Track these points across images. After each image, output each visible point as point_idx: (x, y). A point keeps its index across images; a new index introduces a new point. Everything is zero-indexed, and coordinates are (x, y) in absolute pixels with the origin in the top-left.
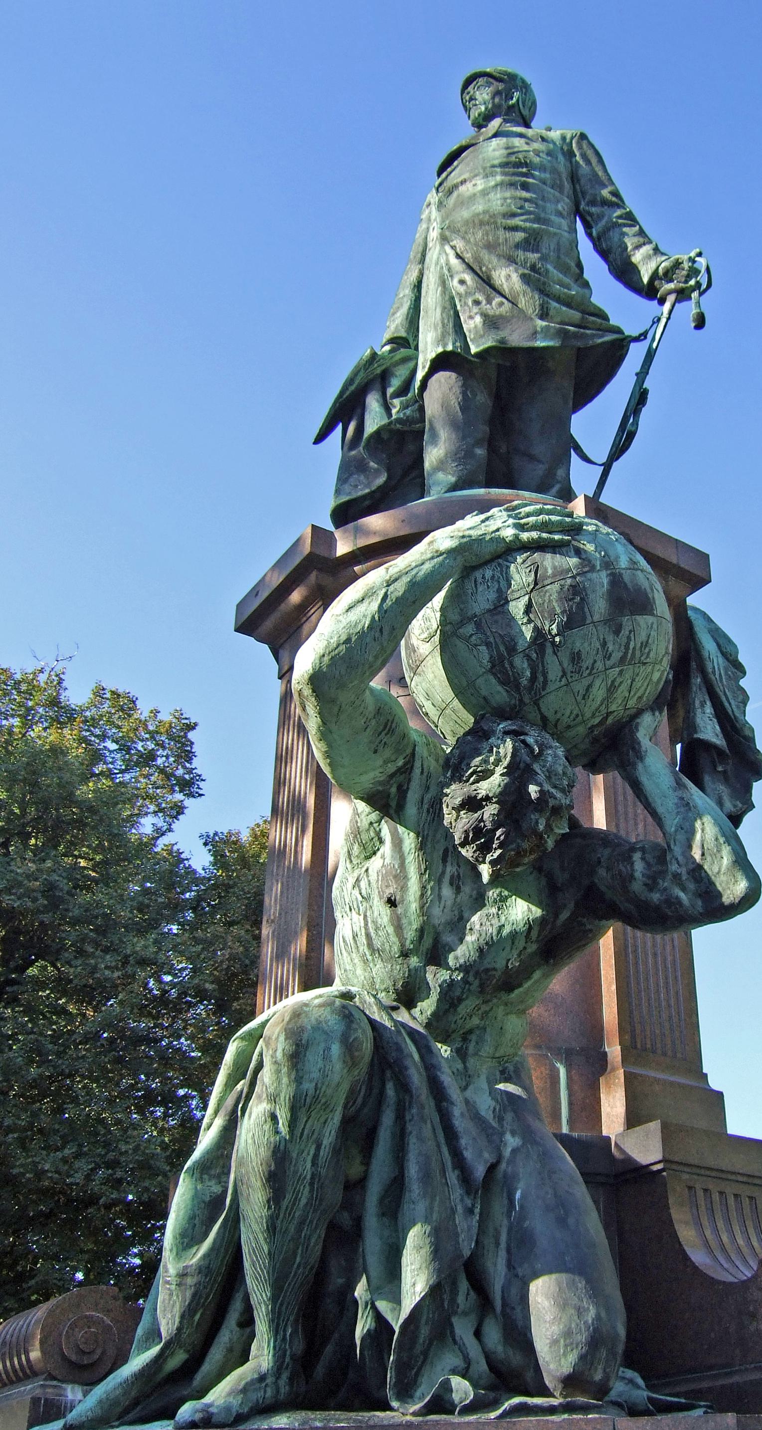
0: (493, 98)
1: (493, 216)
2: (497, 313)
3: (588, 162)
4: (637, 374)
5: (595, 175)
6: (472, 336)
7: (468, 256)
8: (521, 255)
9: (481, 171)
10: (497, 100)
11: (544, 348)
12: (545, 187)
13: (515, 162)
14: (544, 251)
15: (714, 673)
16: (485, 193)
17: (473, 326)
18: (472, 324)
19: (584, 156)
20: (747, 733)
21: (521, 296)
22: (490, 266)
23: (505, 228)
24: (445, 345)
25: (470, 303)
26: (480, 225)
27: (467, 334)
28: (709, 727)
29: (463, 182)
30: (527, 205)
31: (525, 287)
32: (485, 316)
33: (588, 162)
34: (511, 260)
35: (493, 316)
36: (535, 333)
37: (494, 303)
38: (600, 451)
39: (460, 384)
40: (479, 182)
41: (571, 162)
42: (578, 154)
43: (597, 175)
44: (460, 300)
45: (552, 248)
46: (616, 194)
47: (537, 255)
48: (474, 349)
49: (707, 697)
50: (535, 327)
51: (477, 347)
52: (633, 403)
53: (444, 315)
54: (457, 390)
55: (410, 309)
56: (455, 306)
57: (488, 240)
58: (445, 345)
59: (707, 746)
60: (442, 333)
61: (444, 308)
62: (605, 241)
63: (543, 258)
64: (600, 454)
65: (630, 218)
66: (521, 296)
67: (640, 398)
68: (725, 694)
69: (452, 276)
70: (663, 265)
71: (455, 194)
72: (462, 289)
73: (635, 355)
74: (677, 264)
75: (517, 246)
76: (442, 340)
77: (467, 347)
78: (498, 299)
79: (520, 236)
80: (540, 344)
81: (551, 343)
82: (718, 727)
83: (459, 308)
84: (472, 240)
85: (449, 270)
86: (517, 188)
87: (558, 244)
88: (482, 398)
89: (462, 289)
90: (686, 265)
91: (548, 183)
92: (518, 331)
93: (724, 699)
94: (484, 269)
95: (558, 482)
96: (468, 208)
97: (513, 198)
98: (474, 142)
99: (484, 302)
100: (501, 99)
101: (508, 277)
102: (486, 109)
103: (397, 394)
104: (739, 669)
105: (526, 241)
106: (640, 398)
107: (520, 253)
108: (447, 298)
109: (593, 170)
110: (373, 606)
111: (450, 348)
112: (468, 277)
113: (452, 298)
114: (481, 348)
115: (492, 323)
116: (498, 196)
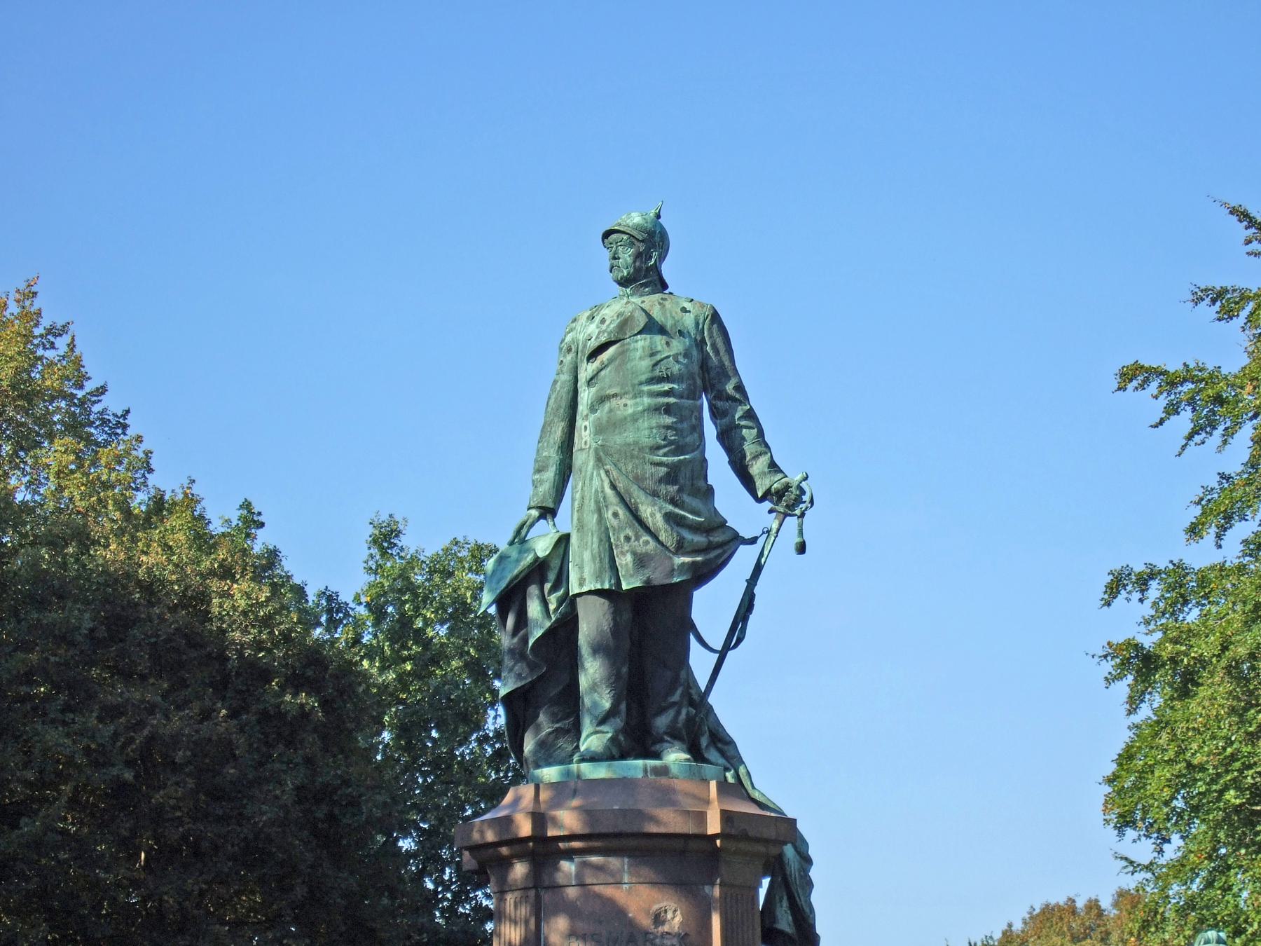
0: (634, 262)
1: (641, 449)
2: (644, 551)
3: (717, 352)
4: (747, 580)
5: (722, 365)
6: (624, 573)
7: (620, 486)
8: (663, 489)
9: (631, 389)
10: (638, 264)
11: (679, 582)
12: (683, 401)
13: (659, 377)
14: (682, 481)
15: (791, 876)
16: (635, 418)
17: (624, 562)
18: (625, 561)
19: (714, 346)
20: (811, 922)
21: (663, 532)
22: (638, 500)
23: (651, 464)
24: (602, 583)
25: (622, 539)
26: (631, 458)
27: (619, 568)
28: (785, 919)
29: (615, 395)
30: (669, 433)
31: (666, 526)
32: (634, 554)
33: (717, 352)
34: (655, 494)
35: (641, 554)
36: (673, 570)
37: (641, 541)
39: (612, 610)
40: (629, 402)
41: (702, 352)
42: (709, 344)
43: (724, 365)
44: (614, 534)
45: (687, 476)
46: (740, 388)
47: (676, 487)
48: (625, 587)
49: (785, 893)
50: (673, 565)
51: (628, 584)
52: (743, 610)
53: (601, 548)
54: (609, 617)
55: (556, 474)
56: (610, 538)
57: (637, 473)
58: (602, 583)
59: (782, 932)
60: (600, 568)
61: (601, 540)
62: (728, 438)
63: (680, 491)
65: (751, 415)
66: (663, 532)
68: (797, 892)
69: (607, 507)
70: (775, 485)
71: (607, 406)
72: (615, 522)
74: (787, 487)
75: (661, 481)
76: (599, 577)
77: (619, 583)
78: (646, 538)
79: (663, 470)
80: (676, 580)
81: (684, 578)
82: (790, 918)
83: (612, 540)
84: (623, 469)
85: (604, 498)
86: (660, 413)
87: (692, 471)
88: (627, 616)
89: (615, 522)
91: (685, 395)
92: (660, 568)
93: (796, 895)
94: (633, 500)
95: (681, 685)
96: (620, 433)
97: (659, 427)
98: (621, 337)
99: (633, 538)
100: (641, 262)
101: (653, 515)
102: (628, 274)
104: (807, 861)
105: (668, 474)
107: (663, 487)
108: (603, 529)
109: (721, 361)
111: (607, 586)
112: (621, 512)
113: (607, 529)
114: (631, 587)
115: (641, 561)
116: (646, 424)
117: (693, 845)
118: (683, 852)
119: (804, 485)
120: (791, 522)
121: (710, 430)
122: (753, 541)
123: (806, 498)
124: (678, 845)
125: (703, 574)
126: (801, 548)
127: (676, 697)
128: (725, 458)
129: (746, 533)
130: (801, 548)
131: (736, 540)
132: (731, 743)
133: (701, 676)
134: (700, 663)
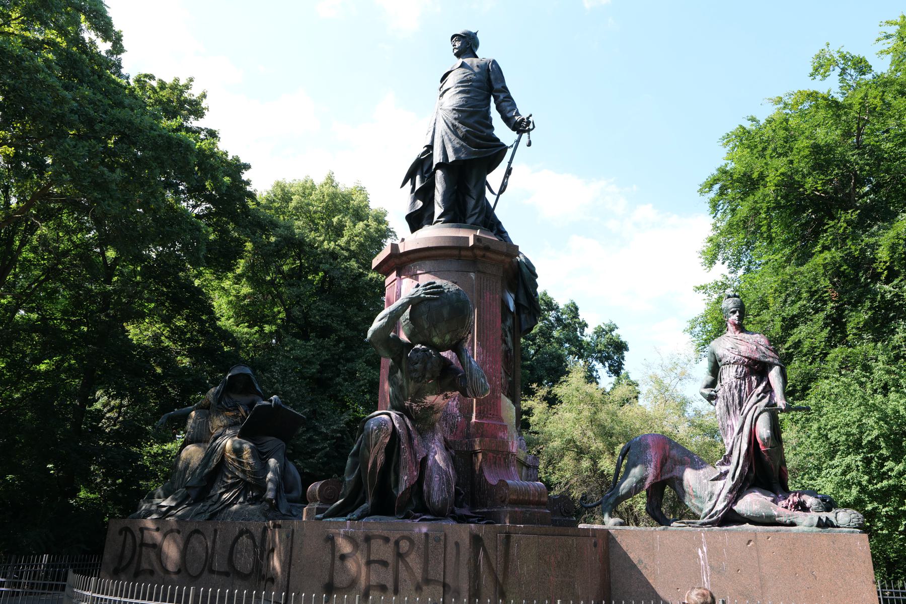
38: (496, 188)
64: (496, 190)
67: (509, 171)
73: (509, 152)
90: (526, 120)
103: (426, 173)
106: (509, 171)
110: (385, 320)
117: (463, 253)
118: (459, 258)
119: (531, 119)
120: (525, 135)
121: (493, 105)
122: (512, 146)
123: (531, 124)
124: (456, 252)
125: (492, 164)
126: (529, 144)
127: (477, 210)
128: (499, 115)
129: (508, 144)
130: (529, 144)
131: (507, 148)
132: (506, 232)
133: (492, 205)
134: (490, 198)
